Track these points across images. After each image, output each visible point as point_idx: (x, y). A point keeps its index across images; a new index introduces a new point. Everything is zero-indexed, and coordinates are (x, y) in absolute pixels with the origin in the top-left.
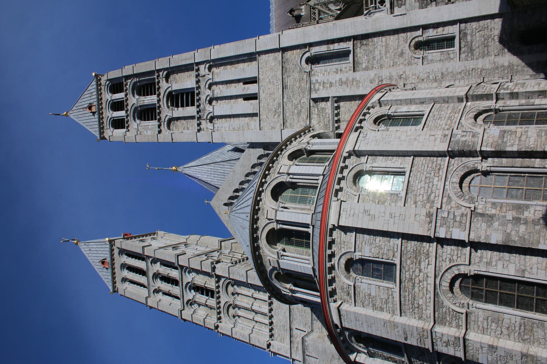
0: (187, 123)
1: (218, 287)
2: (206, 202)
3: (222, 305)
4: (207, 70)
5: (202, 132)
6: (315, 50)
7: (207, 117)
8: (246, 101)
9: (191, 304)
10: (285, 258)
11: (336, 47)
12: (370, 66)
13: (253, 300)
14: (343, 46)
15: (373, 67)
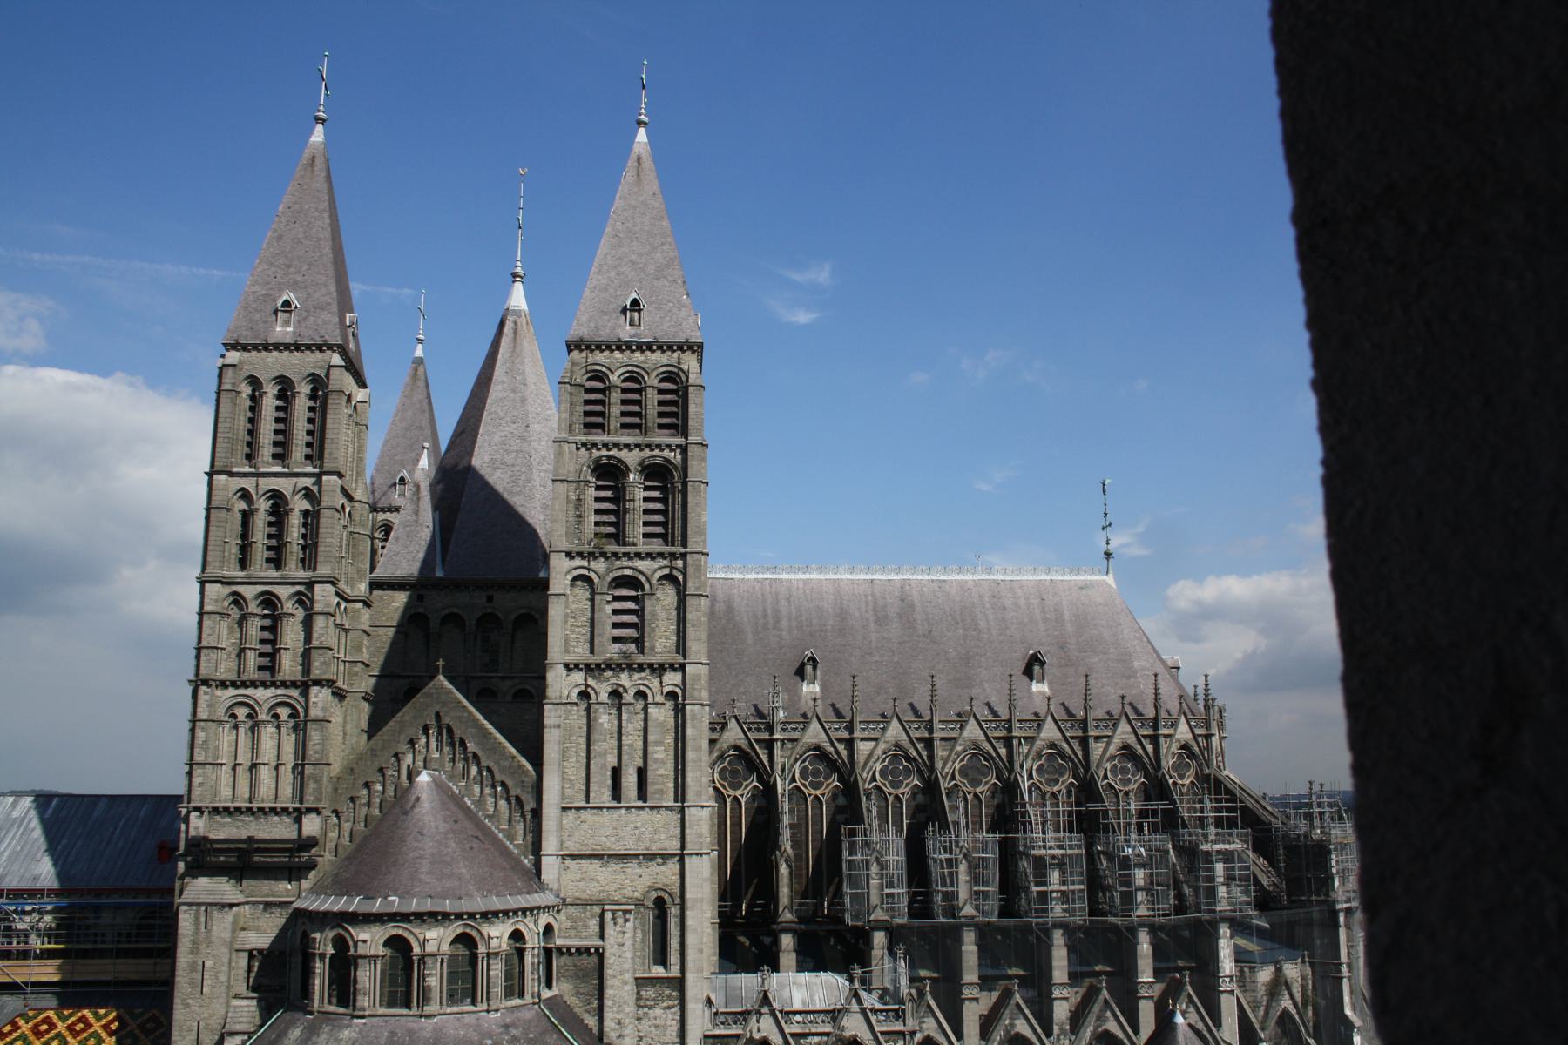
0: (582, 626)
1: (284, 684)
2: (441, 663)
3: (250, 691)
4: (671, 688)
5: (565, 672)
6: (674, 911)
7: (590, 686)
8: (609, 773)
9: (235, 602)
10: (373, 966)
11: (674, 943)
12: (642, 1002)
13: (274, 764)
14: (674, 958)
15: (639, 1007)
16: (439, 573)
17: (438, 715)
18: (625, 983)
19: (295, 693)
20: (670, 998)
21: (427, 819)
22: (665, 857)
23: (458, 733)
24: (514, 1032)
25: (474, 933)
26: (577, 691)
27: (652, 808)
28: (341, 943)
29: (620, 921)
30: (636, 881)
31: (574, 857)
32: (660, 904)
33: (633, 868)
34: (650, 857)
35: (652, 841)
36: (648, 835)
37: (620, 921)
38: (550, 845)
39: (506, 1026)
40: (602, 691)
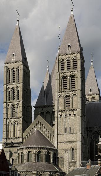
3: (11, 120)
14: (75, 158)
16: (46, 104)
17: (39, 121)
18: (67, 162)
19: (18, 119)
20: (74, 165)
21: (35, 135)
22: (74, 142)
23: (42, 124)
24: (47, 166)
25: (41, 151)
26: (60, 115)
27: (72, 134)
28: (22, 153)
29: (67, 152)
30: (69, 146)
31: (60, 142)
32: (73, 149)
33: (69, 144)
34: (71, 142)
35: (72, 139)
36: (71, 138)
37: (67, 152)
38: (55, 140)
39: (46, 165)
40: (63, 115)
